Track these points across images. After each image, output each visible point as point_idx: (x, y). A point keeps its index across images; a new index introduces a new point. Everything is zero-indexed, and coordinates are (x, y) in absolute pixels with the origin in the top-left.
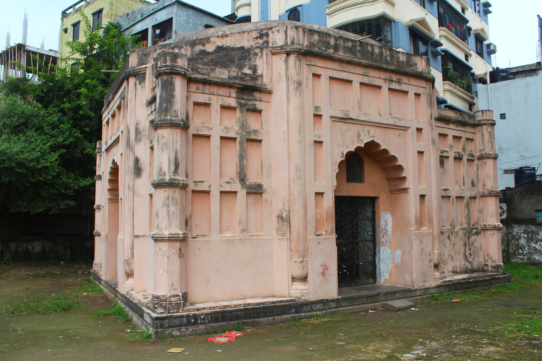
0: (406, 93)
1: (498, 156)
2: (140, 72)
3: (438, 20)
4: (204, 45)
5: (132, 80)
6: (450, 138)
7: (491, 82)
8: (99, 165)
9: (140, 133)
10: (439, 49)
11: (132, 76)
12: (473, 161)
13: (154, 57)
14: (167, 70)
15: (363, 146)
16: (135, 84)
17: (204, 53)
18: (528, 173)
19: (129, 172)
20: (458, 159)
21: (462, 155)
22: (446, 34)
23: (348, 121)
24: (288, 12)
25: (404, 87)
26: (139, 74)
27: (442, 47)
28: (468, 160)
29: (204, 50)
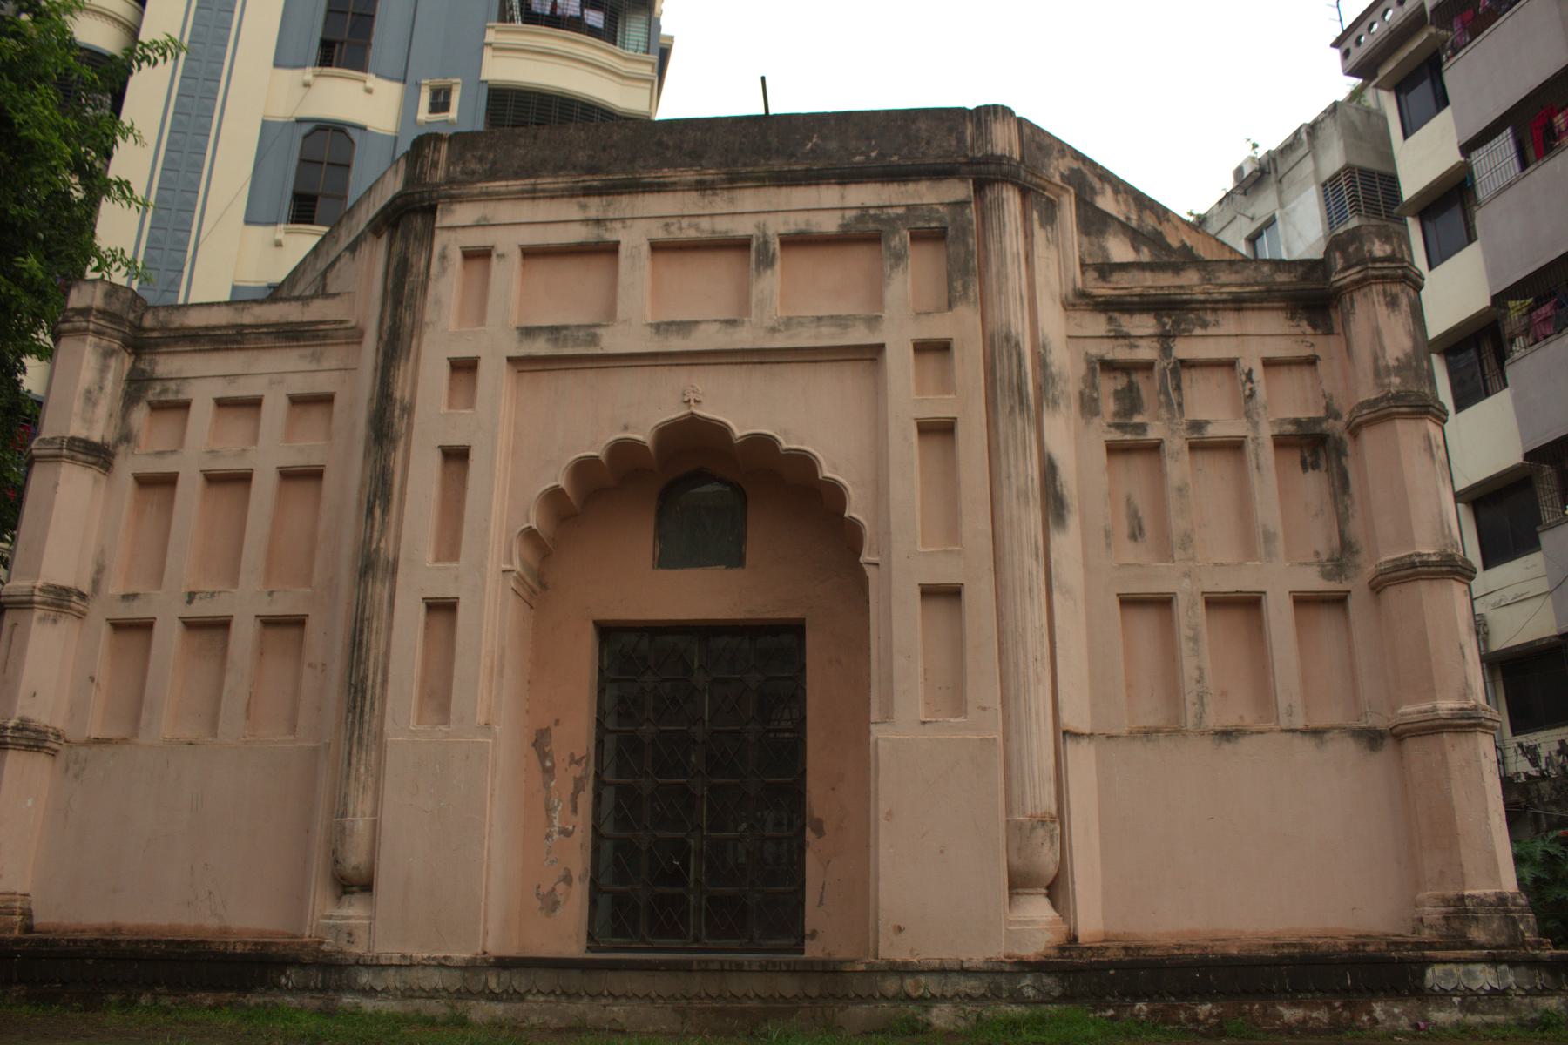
2: (1044, 189)
4: (1160, 223)
8: (89, 392)
9: (1053, 382)
11: (1015, 184)
13: (1062, 169)
16: (1026, 217)
19: (1034, 498)
24: (307, 128)
26: (1037, 192)
29: (1161, 233)
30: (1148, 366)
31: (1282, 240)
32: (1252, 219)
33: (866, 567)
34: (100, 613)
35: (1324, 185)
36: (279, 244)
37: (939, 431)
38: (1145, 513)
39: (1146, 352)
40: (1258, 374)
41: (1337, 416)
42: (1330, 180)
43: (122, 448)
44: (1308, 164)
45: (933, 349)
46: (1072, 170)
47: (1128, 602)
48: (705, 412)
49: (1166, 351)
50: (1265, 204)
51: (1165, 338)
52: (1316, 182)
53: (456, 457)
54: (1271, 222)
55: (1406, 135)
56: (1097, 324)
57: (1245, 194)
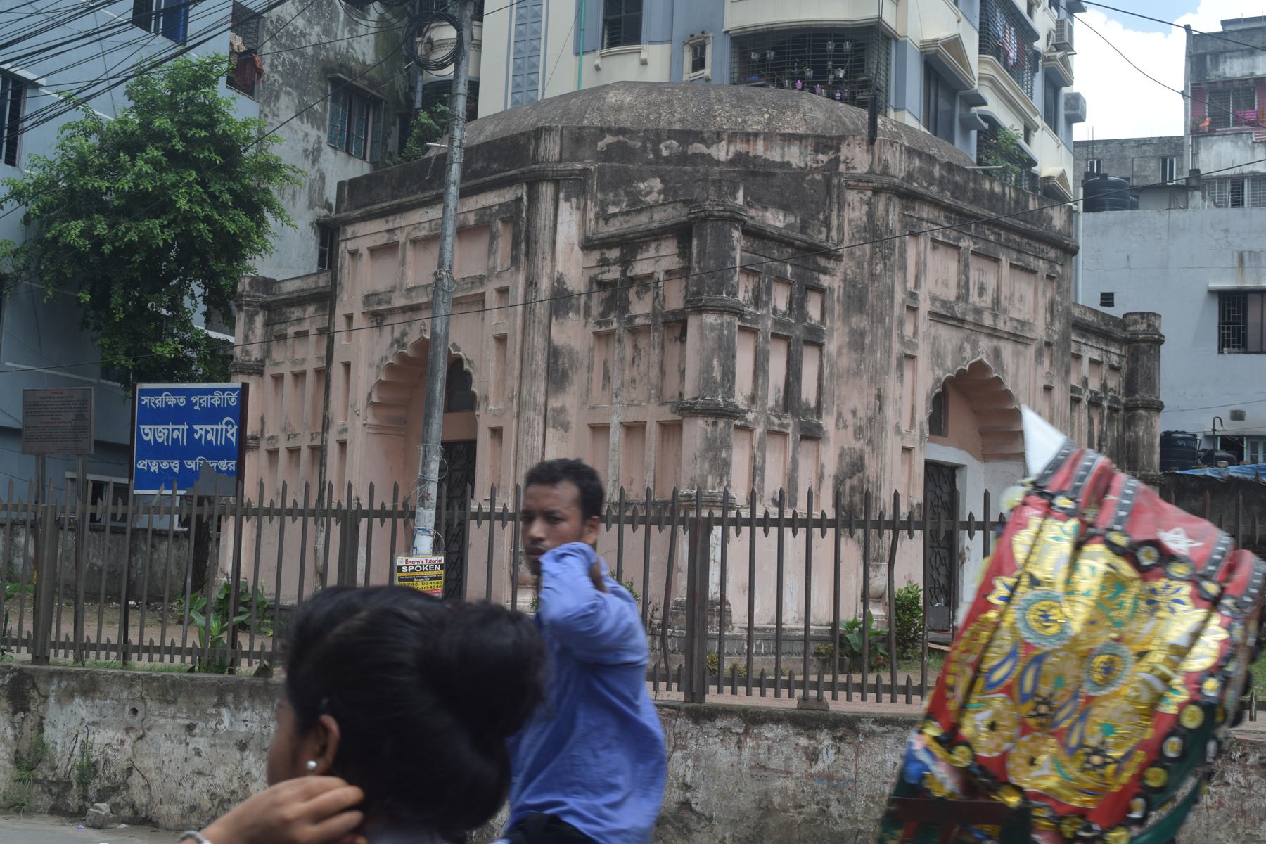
0: (1033, 272)
1: (1163, 407)
3: (980, 33)
4: (708, 147)
5: (547, 190)
6: (1085, 361)
7: (1086, 210)
10: (975, 109)
12: (1117, 411)
14: (725, 210)
15: (967, 368)
17: (708, 159)
18: (1182, 446)
20: (1095, 403)
21: (1101, 399)
22: (993, 73)
23: (950, 322)
25: (1032, 262)
27: (983, 108)
28: (1109, 407)
36: (597, 68)
37: (501, 340)
39: (614, 273)
43: (267, 361)
46: (608, 146)
47: (595, 428)
51: (625, 262)
53: (347, 366)
56: (596, 255)
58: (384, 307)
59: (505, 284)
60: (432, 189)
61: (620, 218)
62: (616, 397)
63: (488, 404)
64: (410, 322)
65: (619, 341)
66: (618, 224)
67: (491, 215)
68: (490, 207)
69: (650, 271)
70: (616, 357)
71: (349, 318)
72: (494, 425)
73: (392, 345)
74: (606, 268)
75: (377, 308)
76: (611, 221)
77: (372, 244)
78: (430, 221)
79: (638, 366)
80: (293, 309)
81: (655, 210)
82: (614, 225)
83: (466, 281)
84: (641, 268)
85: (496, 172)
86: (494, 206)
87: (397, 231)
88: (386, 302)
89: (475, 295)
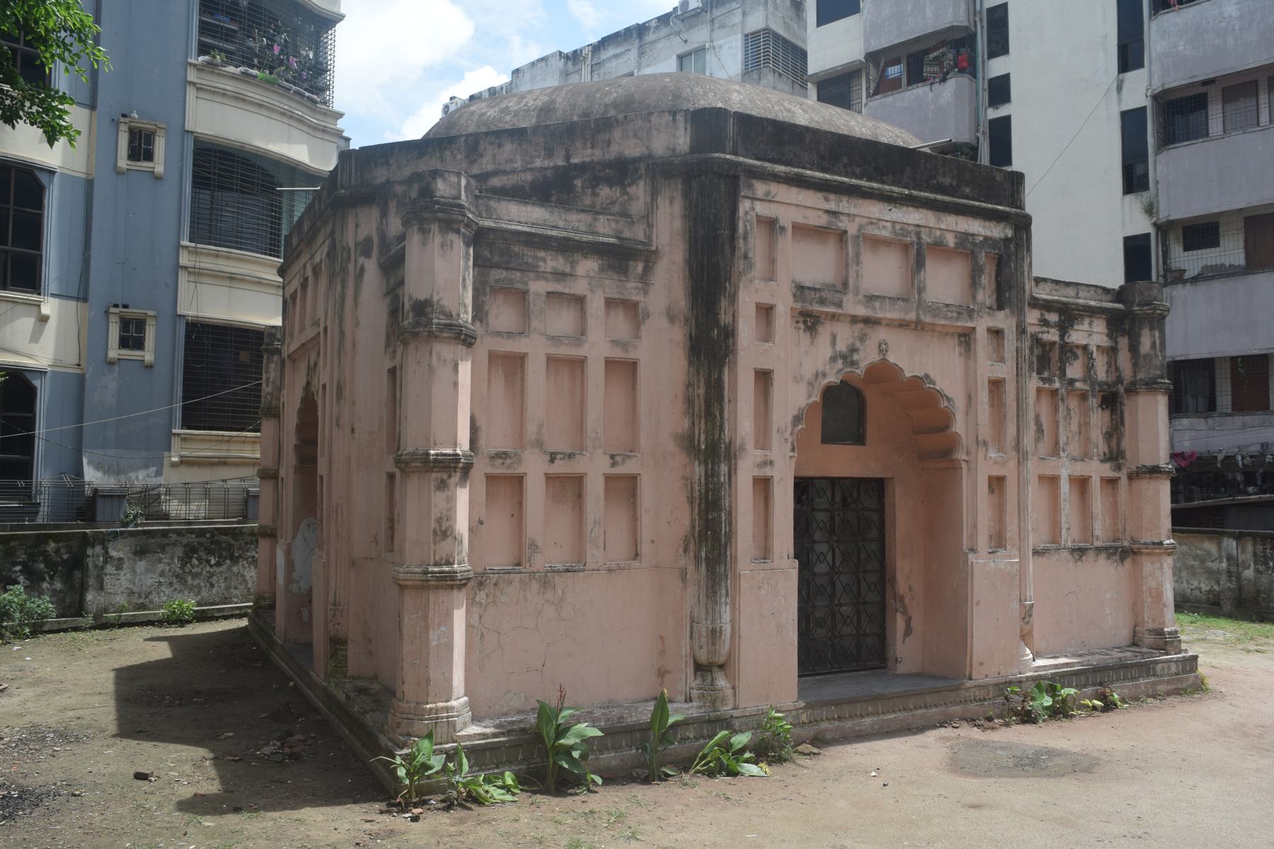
30: (1054, 343)
31: (708, 65)
32: (686, 42)
33: (962, 462)
34: (481, 468)
35: (746, 36)
37: (996, 385)
38: (1045, 427)
39: (1052, 336)
40: (1095, 355)
41: (1122, 383)
42: (752, 34)
44: (738, 18)
45: (997, 333)
48: (891, 358)
49: (1062, 337)
50: (699, 36)
51: (1064, 328)
52: (743, 29)
53: (764, 377)
54: (701, 50)
55: (820, 22)
57: (683, 21)
58: (832, 309)
59: (999, 325)
60: (883, 182)
61: (1051, 285)
62: (1064, 451)
63: (987, 450)
64: (863, 338)
65: (1062, 400)
66: (1048, 290)
67: (974, 244)
68: (973, 235)
69: (1084, 342)
70: (1061, 415)
71: (766, 312)
72: (995, 473)
73: (833, 359)
74: (1045, 329)
75: (817, 308)
76: (1042, 284)
77: (800, 220)
78: (894, 223)
79: (1070, 425)
80: (542, 254)
81: (1079, 287)
82: (1044, 290)
83: (950, 308)
84: (1077, 336)
85: (967, 197)
86: (978, 235)
87: (842, 218)
88: (834, 304)
89: (957, 327)
